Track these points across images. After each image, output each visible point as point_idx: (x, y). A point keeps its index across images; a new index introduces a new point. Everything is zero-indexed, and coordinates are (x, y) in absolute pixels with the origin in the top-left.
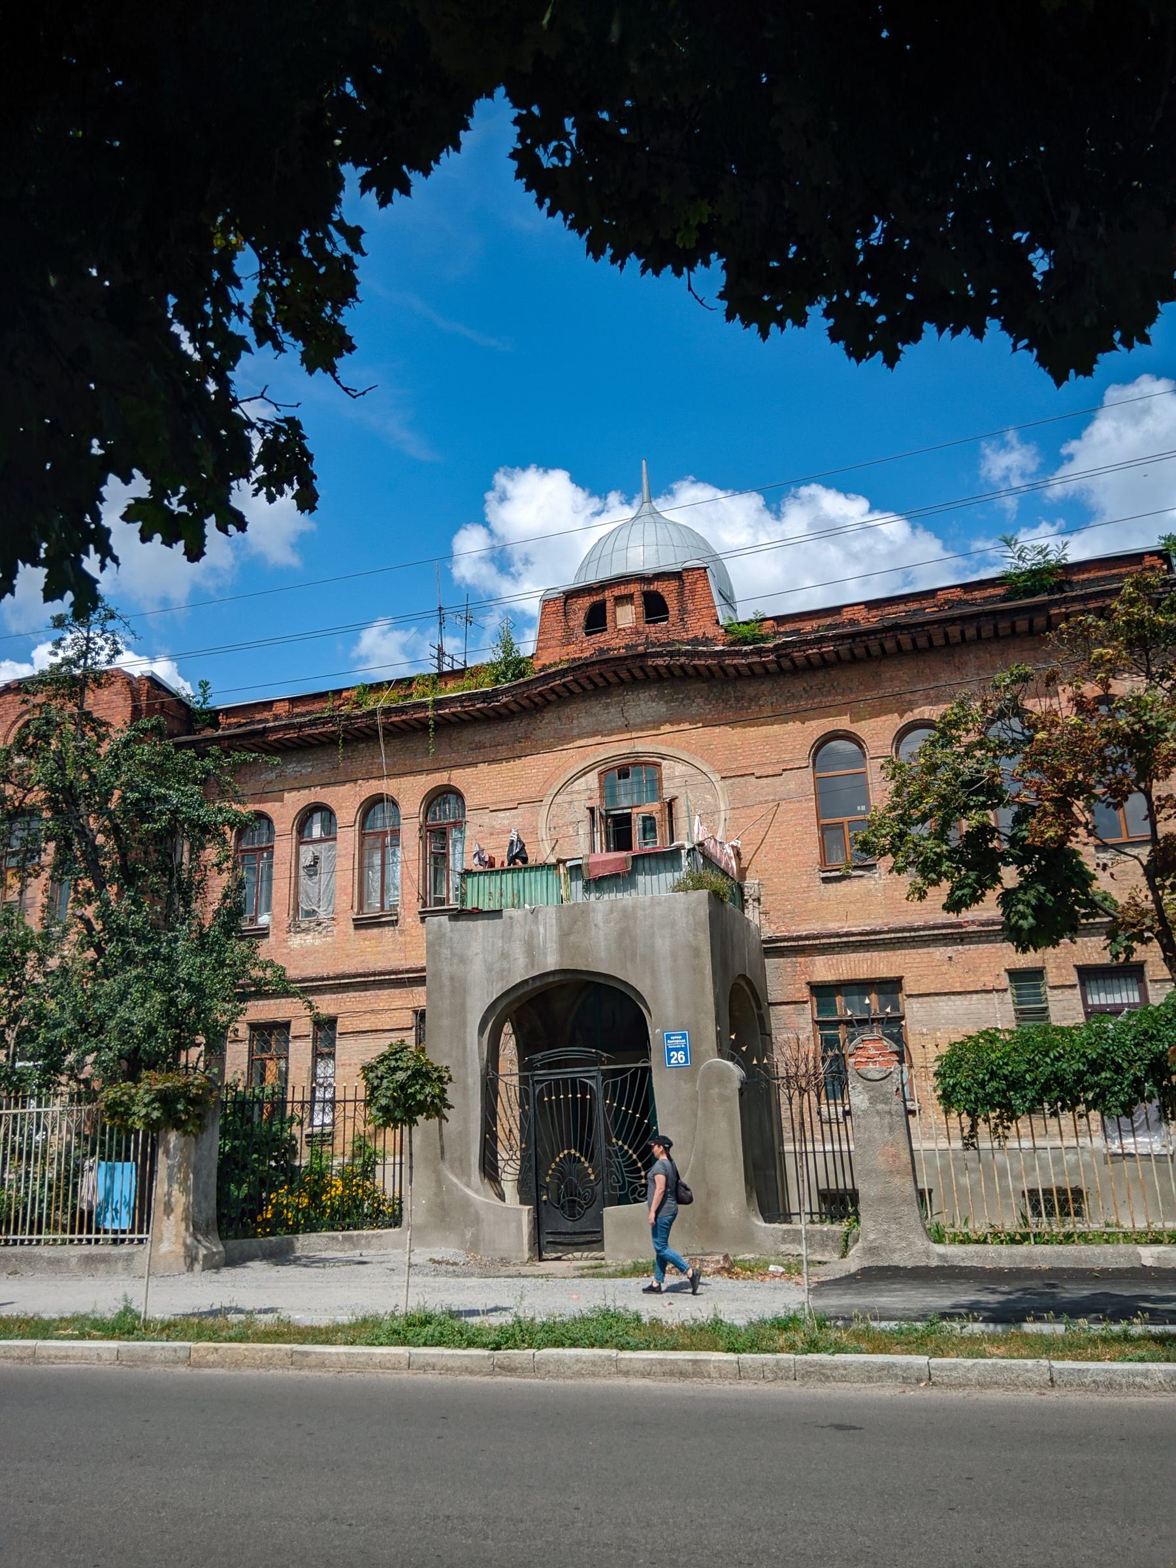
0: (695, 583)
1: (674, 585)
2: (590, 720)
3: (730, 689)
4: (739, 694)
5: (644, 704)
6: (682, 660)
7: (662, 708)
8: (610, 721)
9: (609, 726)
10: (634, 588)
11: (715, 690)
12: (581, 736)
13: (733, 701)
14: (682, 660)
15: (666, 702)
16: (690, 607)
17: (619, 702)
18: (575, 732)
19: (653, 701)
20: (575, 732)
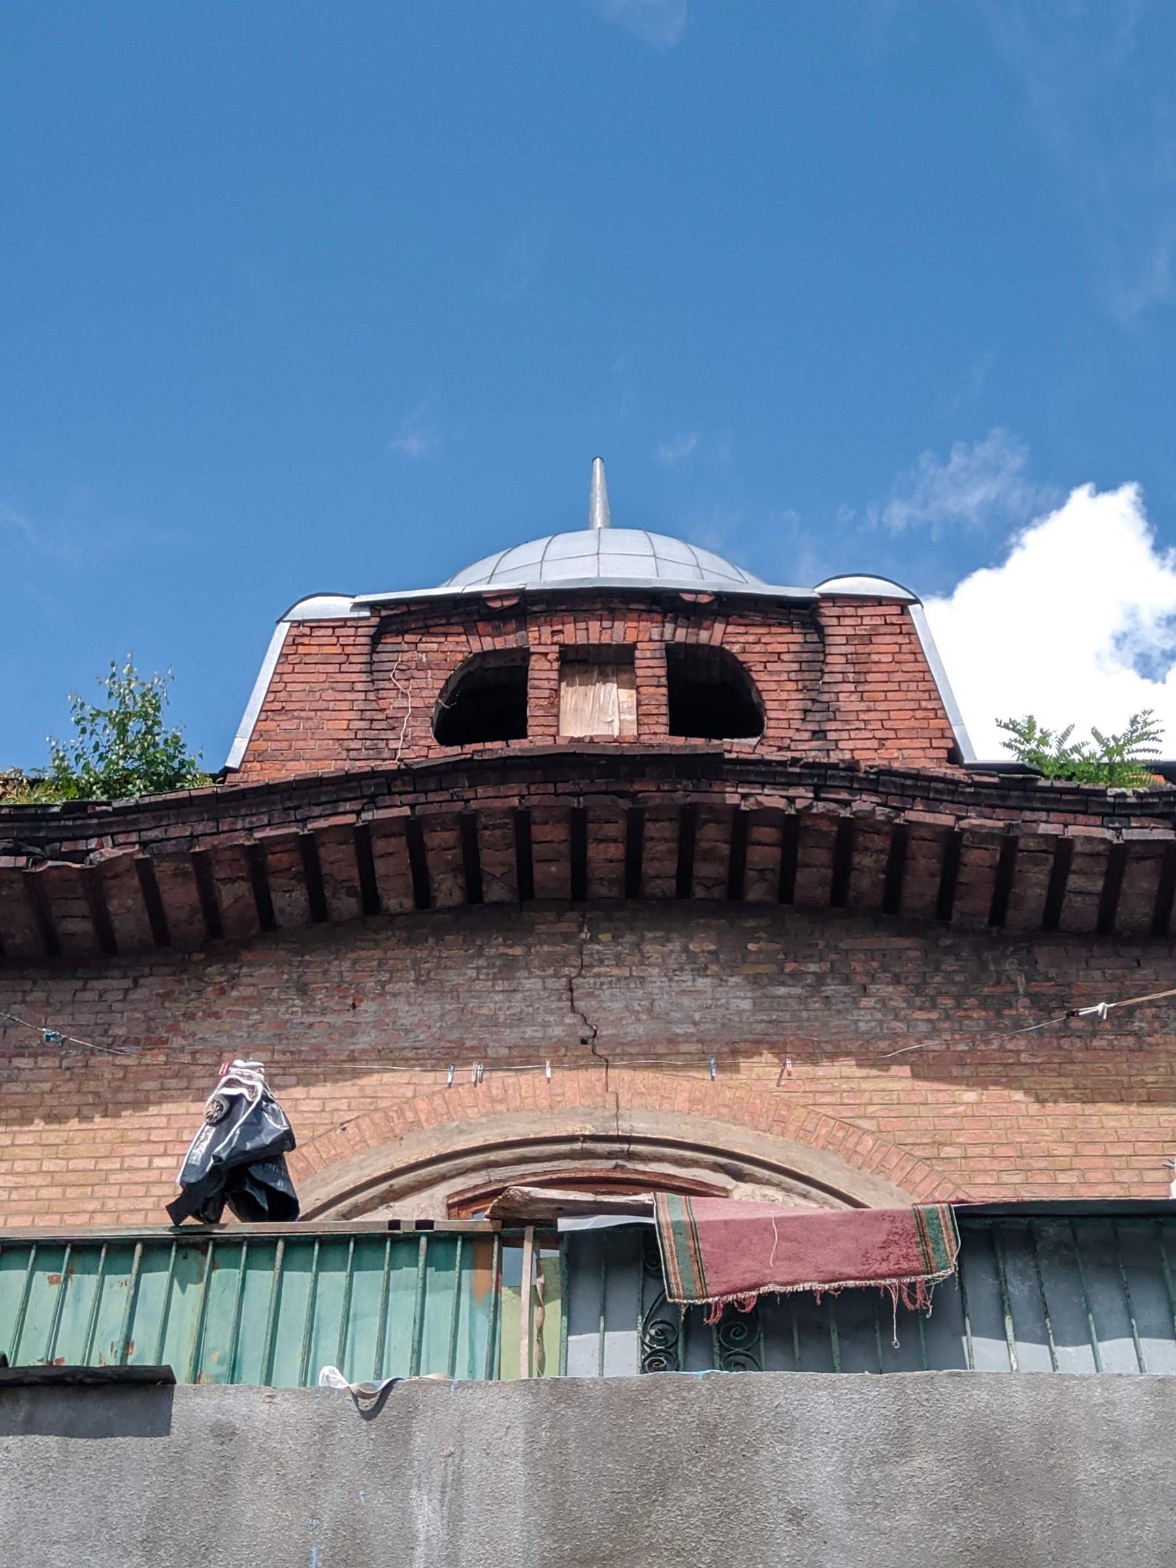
0: (868, 639)
1: (786, 640)
2: (434, 1007)
3: (1010, 966)
4: (1047, 988)
5: (663, 981)
6: (864, 803)
7: (738, 1000)
8: (518, 1020)
9: (510, 1035)
10: (648, 637)
11: (949, 964)
12: (389, 1057)
13: (1022, 1007)
14: (864, 803)
15: (755, 981)
16: (848, 702)
17: (564, 960)
18: (365, 1041)
19: (702, 971)
20: (365, 1041)
